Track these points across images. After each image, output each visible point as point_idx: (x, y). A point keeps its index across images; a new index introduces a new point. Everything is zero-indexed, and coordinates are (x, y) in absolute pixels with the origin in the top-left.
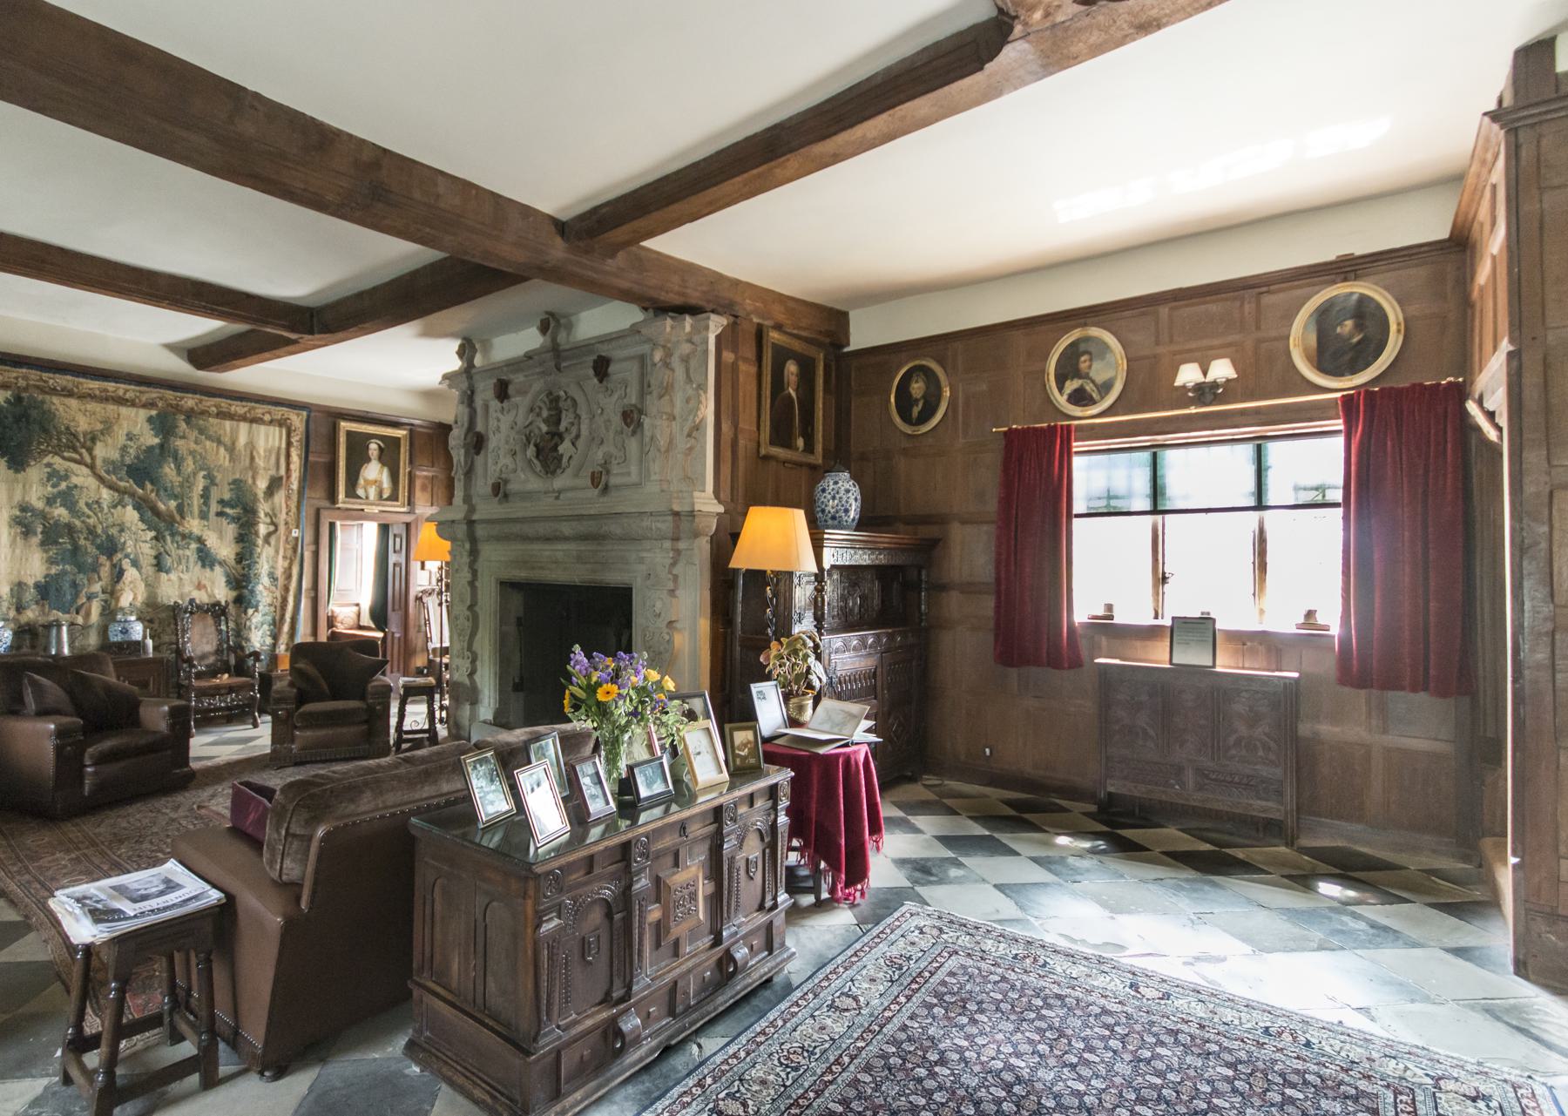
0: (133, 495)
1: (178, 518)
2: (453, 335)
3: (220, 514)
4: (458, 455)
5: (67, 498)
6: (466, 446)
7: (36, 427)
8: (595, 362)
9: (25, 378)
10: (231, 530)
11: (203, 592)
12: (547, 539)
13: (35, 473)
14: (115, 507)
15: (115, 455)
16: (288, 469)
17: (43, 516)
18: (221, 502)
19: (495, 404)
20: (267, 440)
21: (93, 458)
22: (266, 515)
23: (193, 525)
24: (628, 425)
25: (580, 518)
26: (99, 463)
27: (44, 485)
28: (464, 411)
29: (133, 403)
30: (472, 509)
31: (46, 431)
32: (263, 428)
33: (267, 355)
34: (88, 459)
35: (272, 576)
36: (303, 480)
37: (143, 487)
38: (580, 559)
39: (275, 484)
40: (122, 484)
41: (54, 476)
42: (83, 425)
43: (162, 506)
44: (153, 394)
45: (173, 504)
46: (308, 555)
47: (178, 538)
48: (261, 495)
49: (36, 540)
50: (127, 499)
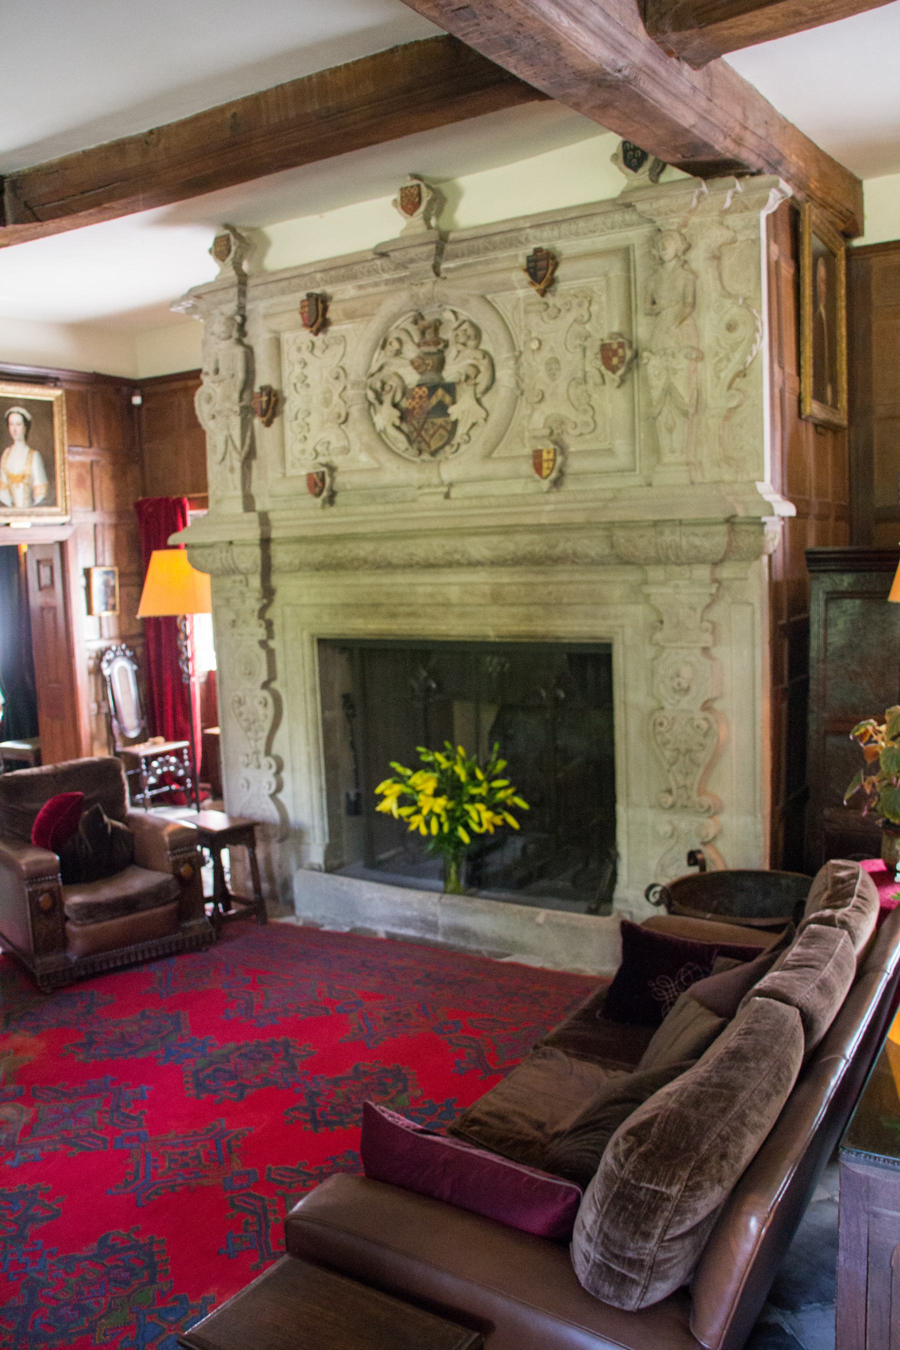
2: (205, 221)
8: (529, 260)
12: (430, 566)
19: (297, 337)
24: (613, 370)
25: (507, 531)
38: (497, 597)
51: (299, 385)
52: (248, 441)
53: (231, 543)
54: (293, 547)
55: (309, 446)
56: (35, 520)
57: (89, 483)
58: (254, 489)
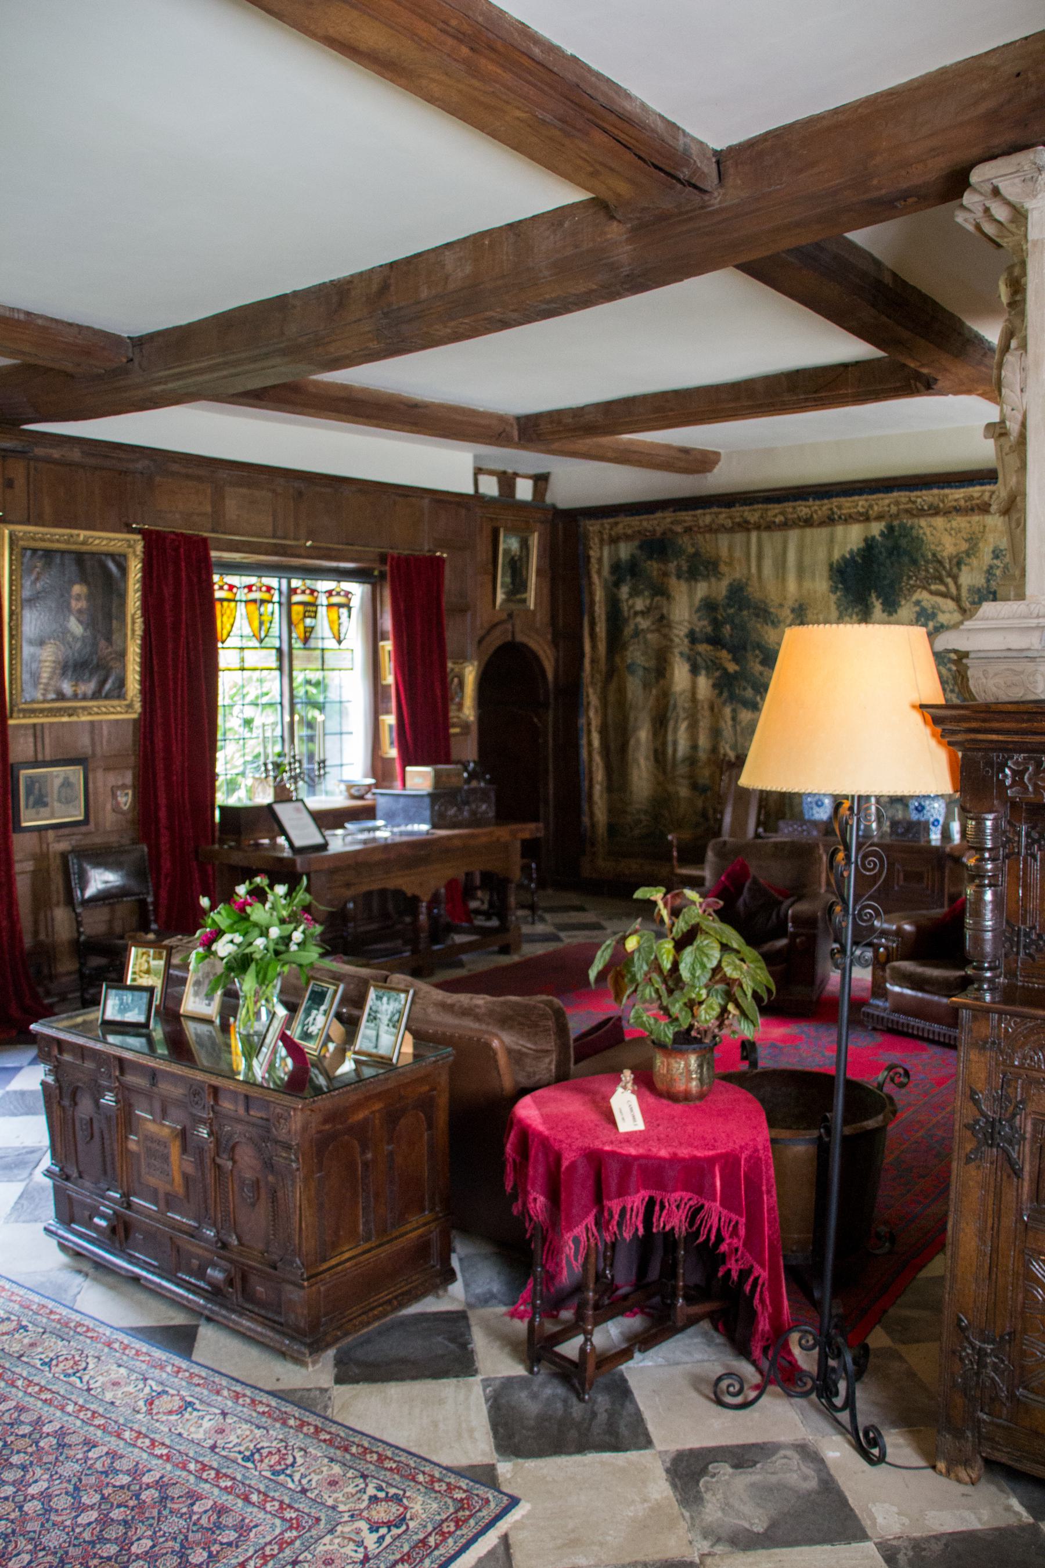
9: (897, 503)
21: (958, 587)
26: (964, 593)
31: (914, 562)
34: (953, 590)
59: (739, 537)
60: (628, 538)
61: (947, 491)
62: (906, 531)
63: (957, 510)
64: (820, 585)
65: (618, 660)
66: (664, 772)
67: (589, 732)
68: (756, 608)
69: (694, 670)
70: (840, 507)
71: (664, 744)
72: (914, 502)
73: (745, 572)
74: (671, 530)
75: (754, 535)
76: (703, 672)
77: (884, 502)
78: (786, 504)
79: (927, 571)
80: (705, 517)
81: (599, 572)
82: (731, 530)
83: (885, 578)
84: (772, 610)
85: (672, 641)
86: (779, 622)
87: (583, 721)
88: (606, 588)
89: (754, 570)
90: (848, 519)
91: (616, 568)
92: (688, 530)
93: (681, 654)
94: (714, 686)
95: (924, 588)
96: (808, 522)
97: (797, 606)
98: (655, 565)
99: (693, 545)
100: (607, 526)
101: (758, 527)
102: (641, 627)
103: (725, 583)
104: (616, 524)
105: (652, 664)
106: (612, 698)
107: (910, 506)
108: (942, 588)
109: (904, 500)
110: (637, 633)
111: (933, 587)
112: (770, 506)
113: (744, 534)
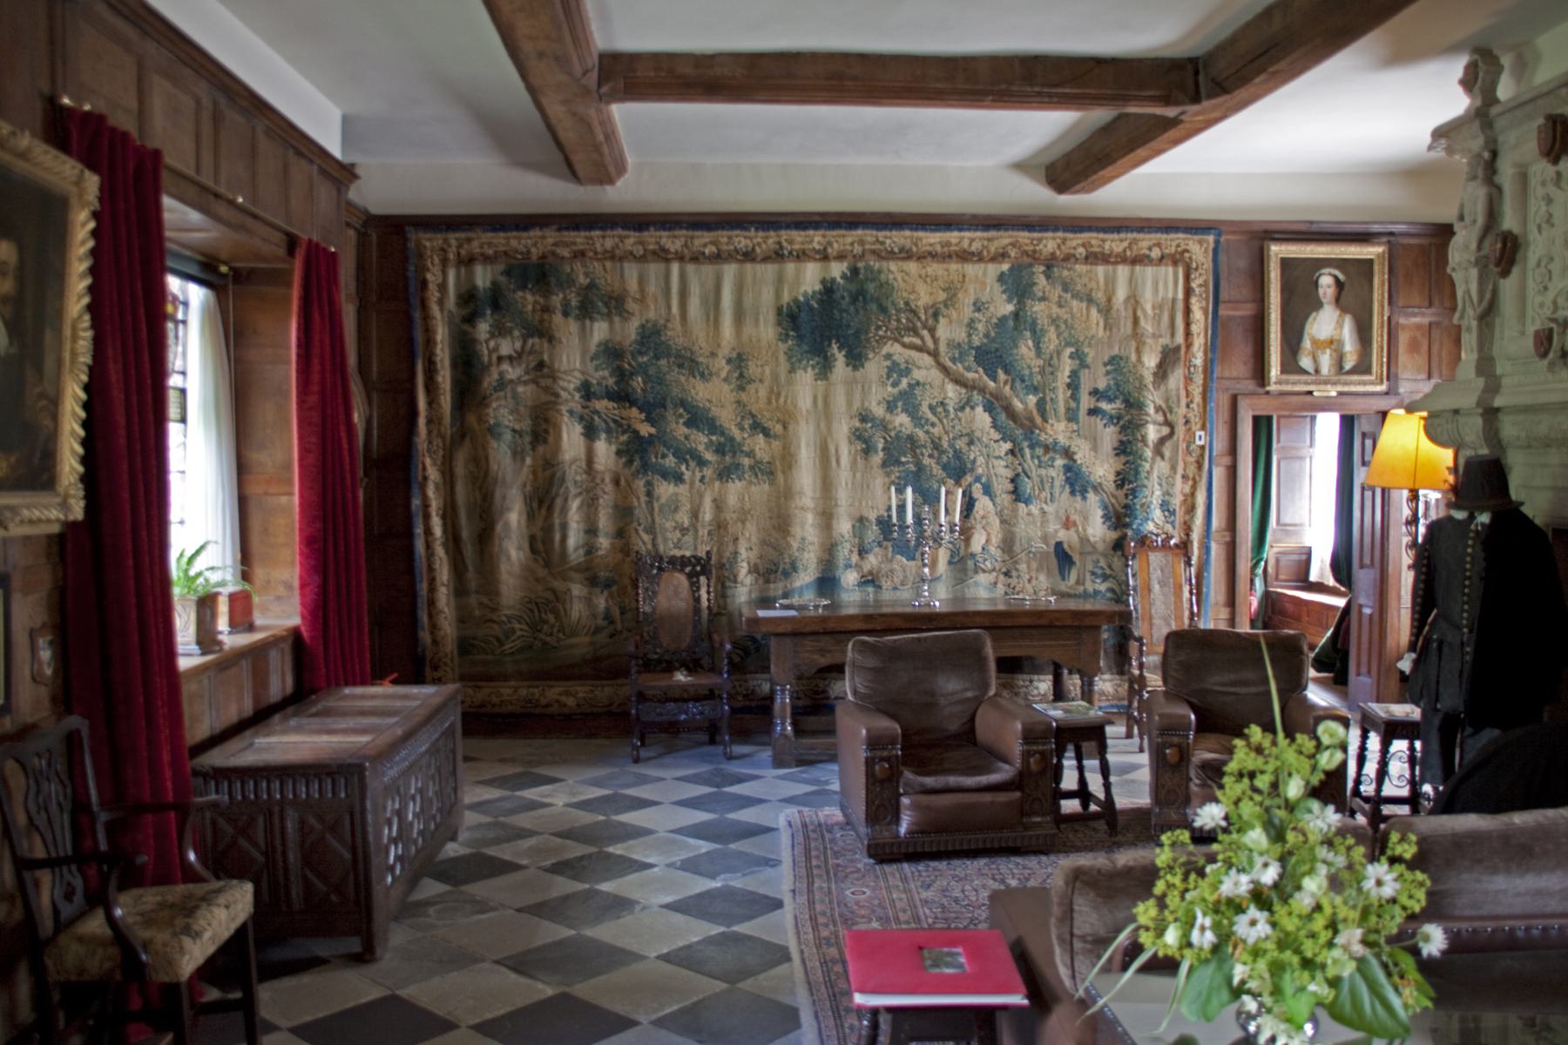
0: (982, 390)
1: (1038, 420)
2: (1451, 49)
3: (1093, 412)
4: (1466, 281)
5: (907, 401)
6: (1481, 263)
7: (874, 307)
10: (1109, 436)
11: (1072, 532)
13: (874, 367)
14: (962, 409)
15: (960, 335)
16: (1188, 334)
17: (884, 426)
18: (1095, 393)
20: (1156, 290)
22: (1158, 409)
23: (1058, 430)
26: (943, 348)
27: (884, 384)
28: (1478, 194)
29: (978, 257)
30: (1493, 386)
31: (883, 310)
32: (1149, 270)
33: (1141, 152)
34: (930, 344)
35: (1165, 506)
36: (1211, 348)
37: (994, 379)
39: (1169, 358)
40: (970, 375)
41: (896, 371)
42: (924, 297)
43: (1018, 405)
44: (1003, 239)
45: (1032, 400)
46: (1219, 474)
47: (1040, 451)
48: (1149, 378)
49: (877, 458)
50: (977, 397)
51: (1544, 226)
52: (1488, 296)
53: (1456, 412)
54: (1521, 417)
55: (1551, 295)
56: (1340, 388)
57: (1425, 347)
58: (1496, 352)
59: (654, 269)
60: (487, 259)
61: (921, 234)
62: (874, 275)
63: (933, 255)
64: (766, 331)
65: (471, 419)
66: (547, 564)
67: (427, 517)
68: (678, 356)
69: (590, 433)
70: (791, 242)
71: (548, 529)
72: (882, 243)
73: (663, 312)
74: (554, 254)
75: (675, 267)
76: (603, 436)
77: (846, 239)
78: (720, 232)
79: (898, 321)
80: (606, 241)
81: (441, 302)
82: (642, 259)
83: (848, 326)
84: (701, 359)
85: (557, 395)
86: (711, 374)
87: (416, 502)
88: (450, 323)
89: (675, 309)
90: (801, 256)
91: (468, 297)
92: (580, 255)
93: (571, 412)
94: (619, 453)
95: (896, 340)
96: (748, 256)
97: (734, 355)
98: (530, 298)
99: (586, 274)
100: (454, 242)
101: (681, 258)
102: (508, 377)
103: (633, 327)
104: (469, 240)
105: (526, 425)
106: (460, 469)
107: (878, 246)
108: (917, 341)
109: (869, 239)
110: (502, 384)
111: (906, 340)
112: (699, 233)
113: (662, 266)
